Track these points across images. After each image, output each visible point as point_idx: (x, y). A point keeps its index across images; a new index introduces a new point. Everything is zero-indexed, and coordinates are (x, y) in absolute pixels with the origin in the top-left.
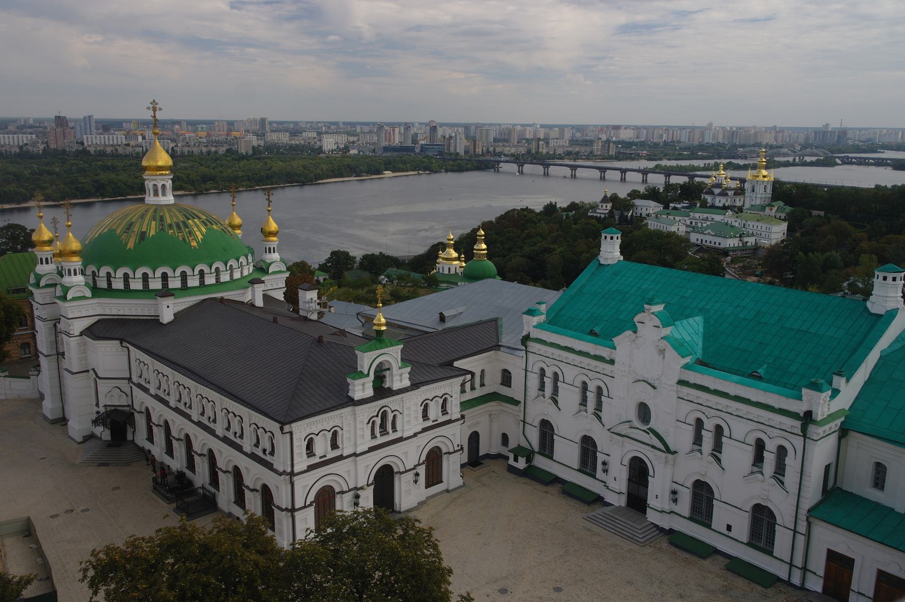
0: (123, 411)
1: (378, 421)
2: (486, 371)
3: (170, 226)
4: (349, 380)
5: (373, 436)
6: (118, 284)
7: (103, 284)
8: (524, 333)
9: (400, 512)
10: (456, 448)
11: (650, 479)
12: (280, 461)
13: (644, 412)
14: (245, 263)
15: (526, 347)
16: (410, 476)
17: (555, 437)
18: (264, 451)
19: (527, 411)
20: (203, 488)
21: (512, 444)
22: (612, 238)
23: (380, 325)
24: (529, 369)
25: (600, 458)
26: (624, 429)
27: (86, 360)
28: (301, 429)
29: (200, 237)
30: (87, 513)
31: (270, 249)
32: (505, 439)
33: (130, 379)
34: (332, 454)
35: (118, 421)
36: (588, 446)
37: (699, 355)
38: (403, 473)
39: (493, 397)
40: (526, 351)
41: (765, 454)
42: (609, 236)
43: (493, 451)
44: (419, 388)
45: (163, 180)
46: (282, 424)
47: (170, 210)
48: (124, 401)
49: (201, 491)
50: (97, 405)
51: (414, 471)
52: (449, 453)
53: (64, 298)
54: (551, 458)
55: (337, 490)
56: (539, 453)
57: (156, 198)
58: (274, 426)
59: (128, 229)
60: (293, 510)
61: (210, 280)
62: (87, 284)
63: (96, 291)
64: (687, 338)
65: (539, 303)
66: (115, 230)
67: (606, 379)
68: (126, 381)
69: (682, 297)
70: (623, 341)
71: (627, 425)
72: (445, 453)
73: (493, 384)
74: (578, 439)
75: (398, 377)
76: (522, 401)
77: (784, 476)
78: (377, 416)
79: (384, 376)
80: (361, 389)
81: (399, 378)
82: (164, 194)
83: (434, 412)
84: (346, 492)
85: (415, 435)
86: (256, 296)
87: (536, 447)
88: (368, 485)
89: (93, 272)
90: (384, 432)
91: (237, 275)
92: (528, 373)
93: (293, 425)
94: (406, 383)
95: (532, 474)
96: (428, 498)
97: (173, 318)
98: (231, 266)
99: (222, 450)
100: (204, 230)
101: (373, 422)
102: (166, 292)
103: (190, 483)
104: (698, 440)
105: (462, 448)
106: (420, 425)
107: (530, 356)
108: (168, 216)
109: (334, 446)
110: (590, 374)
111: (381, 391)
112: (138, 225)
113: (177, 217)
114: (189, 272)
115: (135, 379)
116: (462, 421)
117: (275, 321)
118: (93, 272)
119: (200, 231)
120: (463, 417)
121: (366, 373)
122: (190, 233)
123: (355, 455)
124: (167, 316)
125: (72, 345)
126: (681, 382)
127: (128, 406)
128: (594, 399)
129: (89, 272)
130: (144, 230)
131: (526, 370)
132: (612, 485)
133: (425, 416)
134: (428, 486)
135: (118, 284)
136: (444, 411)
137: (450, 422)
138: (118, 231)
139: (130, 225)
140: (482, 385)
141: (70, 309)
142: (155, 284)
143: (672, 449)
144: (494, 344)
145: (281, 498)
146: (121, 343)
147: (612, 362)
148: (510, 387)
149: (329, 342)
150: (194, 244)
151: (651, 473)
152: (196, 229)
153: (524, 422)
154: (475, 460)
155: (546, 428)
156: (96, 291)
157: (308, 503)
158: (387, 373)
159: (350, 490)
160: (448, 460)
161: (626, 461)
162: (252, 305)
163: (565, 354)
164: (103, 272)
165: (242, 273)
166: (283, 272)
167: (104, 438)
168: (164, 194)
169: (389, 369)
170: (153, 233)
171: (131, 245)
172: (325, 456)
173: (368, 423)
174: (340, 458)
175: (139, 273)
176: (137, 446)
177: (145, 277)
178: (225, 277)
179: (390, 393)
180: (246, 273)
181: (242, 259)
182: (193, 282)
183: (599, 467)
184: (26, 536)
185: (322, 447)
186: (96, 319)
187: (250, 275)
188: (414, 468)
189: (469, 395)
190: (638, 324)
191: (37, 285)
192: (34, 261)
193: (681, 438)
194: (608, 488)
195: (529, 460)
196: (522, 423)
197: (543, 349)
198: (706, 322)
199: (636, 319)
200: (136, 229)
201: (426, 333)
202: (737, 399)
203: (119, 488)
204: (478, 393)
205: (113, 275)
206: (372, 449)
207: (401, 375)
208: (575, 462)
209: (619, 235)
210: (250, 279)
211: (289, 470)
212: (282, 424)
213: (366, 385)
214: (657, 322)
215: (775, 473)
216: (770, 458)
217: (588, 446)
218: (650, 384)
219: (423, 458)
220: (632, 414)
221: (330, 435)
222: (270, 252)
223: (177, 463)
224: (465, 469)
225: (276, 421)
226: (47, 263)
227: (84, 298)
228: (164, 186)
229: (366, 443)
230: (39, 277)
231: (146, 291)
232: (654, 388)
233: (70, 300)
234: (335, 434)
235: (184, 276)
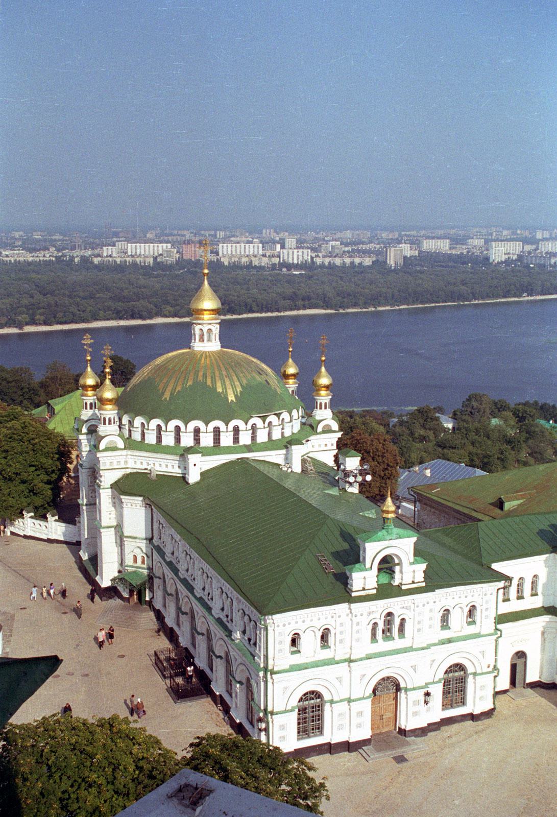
6: (151, 439)
7: (137, 436)
10: (486, 670)
18: (250, 640)
23: (388, 512)
44: (433, 591)
57: (202, 344)
63: (130, 444)
91: (276, 435)
98: (270, 423)
99: (217, 632)
124: (194, 477)
137: (477, 636)
141: (105, 459)
166: (335, 432)
168: (209, 340)
181: (285, 415)
182: (226, 440)
206: (369, 657)
228: (210, 330)
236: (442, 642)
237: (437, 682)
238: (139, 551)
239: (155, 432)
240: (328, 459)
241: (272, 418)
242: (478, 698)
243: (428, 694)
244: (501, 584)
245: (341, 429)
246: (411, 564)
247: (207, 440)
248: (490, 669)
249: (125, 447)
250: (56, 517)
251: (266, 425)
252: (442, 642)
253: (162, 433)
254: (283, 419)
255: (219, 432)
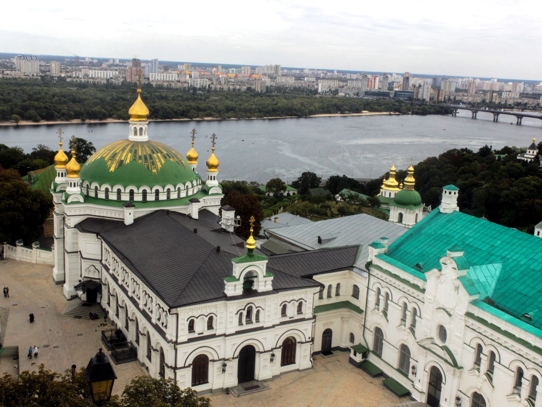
0: (95, 282)
1: (245, 313)
2: (341, 285)
3: (140, 158)
4: (225, 282)
5: (240, 323)
6: (102, 195)
8: (369, 260)
9: (257, 381)
10: (307, 340)
11: (442, 385)
12: (170, 334)
13: (442, 332)
14: (190, 186)
15: (369, 270)
16: (268, 356)
17: (384, 342)
18: (163, 324)
19: (367, 318)
20: (131, 343)
21: (356, 343)
22: (450, 193)
24: (370, 287)
25: (412, 363)
26: (428, 344)
27: (77, 244)
28: (185, 313)
29: (159, 166)
30: (56, 349)
31: (211, 177)
32: (352, 337)
33: (101, 261)
34: (208, 333)
35: (92, 289)
36: (405, 351)
37: (490, 294)
38: (262, 352)
39: (346, 304)
40: (369, 274)
41: (523, 380)
42: (448, 192)
43: (343, 345)
44: (278, 292)
45: (141, 124)
46: (171, 307)
47: (142, 146)
48: (96, 276)
49: (130, 345)
50: (81, 276)
51: (271, 353)
52: (302, 343)
53: (66, 202)
54: (380, 356)
55: (210, 358)
56: (373, 352)
58: (166, 308)
59: (113, 157)
60: (175, 368)
61: (163, 197)
62: (82, 194)
63: (87, 199)
64: (482, 279)
65: (383, 239)
66: (104, 158)
67: (420, 304)
68: (99, 262)
69: (492, 246)
70: (432, 275)
71: (429, 342)
72: (298, 343)
73: (346, 295)
74: (398, 346)
75: (263, 283)
76: (364, 310)
77: (535, 399)
78: (244, 309)
79: (253, 282)
80: (233, 288)
81: (264, 283)
82: (141, 134)
83: (292, 311)
84: (216, 361)
85: (273, 326)
86: (194, 210)
87: (371, 347)
88: (233, 358)
89: (88, 185)
90: (249, 321)
91: (183, 195)
92: (370, 291)
93: (179, 309)
94: (270, 288)
95: (365, 367)
96: (282, 374)
97: (132, 222)
98: (179, 188)
100: (163, 161)
101: (241, 314)
102: (130, 204)
103: (125, 338)
104: (478, 361)
105: (313, 340)
106: (279, 319)
107: (372, 278)
108: (140, 150)
109: (210, 326)
110: (409, 298)
111: (249, 290)
112: (119, 155)
113: (146, 150)
114: (148, 190)
115: (103, 262)
116: (313, 321)
117: (195, 231)
118: (88, 185)
119: (160, 161)
120: (314, 317)
121: (237, 278)
122: (153, 163)
123: (225, 335)
124: (129, 220)
125: (69, 233)
126: (469, 315)
127: (99, 279)
128: (411, 318)
129: (85, 185)
130: (123, 159)
131: (368, 288)
132: (417, 385)
133: (284, 313)
134: (283, 364)
135: (102, 195)
136: (299, 311)
138: (106, 159)
139: (115, 155)
140: (337, 294)
142: (125, 197)
143: (459, 364)
144: (350, 265)
145: (169, 360)
146: (97, 236)
147: (423, 291)
148: (357, 298)
149: (224, 252)
150: (154, 171)
151: (444, 381)
152: (157, 161)
153: (364, 327)
154: (327, 349)
155: (379, 333)
156: (87, 199)
157: (187, 364)
158: (255, 280)
159: (219, 360)
160: (301, 347)
161: (428, 369)
162: (189, 217)
163: (393, 280)
164: (93, 186)
165: (187, 193)
167: (82, 299)
169: (256, 277)
170: (128, 161)
171: (112, 169)
172: (202, 333)
173: (237, 314)
174: (213, 336)
175: (115, 189)
176: (102, 307)
177: (119, 192)
178: (174, 196)
179: (255, 294)
180: (190, 193)
181: (188, 184)
182: (151, 198)
183: (411, 370)
184: (15, 359)
185: (201, 327)
186: (86, 217)
187: (194, 195)
188: (272, 350)
189: (326, 301)
190: (442, 265)
191: (55, 190)
192: (54, 174)
193: (466, 358)
194: (414, 387)
195: (365, 355)
196: (363, 327)
197: (380, 274)
198: (504, 268)
199: (441, 261)
200: (117, 158)
201: (307, 250)
202: (506, 334)
203: (81, 335)
204: (334, 300)
205: (99, 189)
207: (266, 282)
208: (395, 363)
209: (457, 192)
210: (190, 198)
211: (174, 340)
212: (171, 307)
213: (237, 287)
214: (455, 265)
215: (529, 396)
216: (526, 385)
217: (405, 351)
218: (447, 312)
219: (280, 343)
220: (434, 334)
221: (207, 319)
222: (211, 179)
223: (120, 324)
224: (317, 356)
225: (168, 305)
226: (62, 176)
227: (78, 202)
229: (235, 327)
230: (56, 185)
231: (119, 202)
232: (450, 315)
233: (70, 204)
234: (211, 319)
235: (145, 193)
236: (282, 323)
237: (278, 348)
238: (93, 268)
239: (104, 192)
240: (215, 211)
241: (180, 185)
242: (303, 357)
243: (273, 355)
244: (318, 289)
245: (223, 192)
246: (264, 277)
247: (138, 198)
248: (310, 340)
249: (85, 201)
250: (38, 246)
251: (176, 189)
252: (282, 323)
253: (109, 193)
254: (187, 186)
255: (146, 193)
